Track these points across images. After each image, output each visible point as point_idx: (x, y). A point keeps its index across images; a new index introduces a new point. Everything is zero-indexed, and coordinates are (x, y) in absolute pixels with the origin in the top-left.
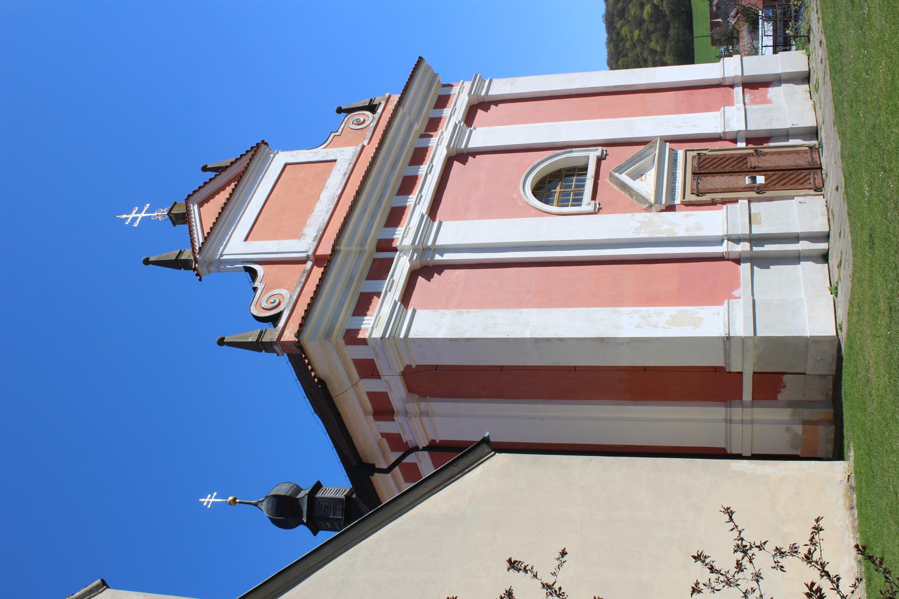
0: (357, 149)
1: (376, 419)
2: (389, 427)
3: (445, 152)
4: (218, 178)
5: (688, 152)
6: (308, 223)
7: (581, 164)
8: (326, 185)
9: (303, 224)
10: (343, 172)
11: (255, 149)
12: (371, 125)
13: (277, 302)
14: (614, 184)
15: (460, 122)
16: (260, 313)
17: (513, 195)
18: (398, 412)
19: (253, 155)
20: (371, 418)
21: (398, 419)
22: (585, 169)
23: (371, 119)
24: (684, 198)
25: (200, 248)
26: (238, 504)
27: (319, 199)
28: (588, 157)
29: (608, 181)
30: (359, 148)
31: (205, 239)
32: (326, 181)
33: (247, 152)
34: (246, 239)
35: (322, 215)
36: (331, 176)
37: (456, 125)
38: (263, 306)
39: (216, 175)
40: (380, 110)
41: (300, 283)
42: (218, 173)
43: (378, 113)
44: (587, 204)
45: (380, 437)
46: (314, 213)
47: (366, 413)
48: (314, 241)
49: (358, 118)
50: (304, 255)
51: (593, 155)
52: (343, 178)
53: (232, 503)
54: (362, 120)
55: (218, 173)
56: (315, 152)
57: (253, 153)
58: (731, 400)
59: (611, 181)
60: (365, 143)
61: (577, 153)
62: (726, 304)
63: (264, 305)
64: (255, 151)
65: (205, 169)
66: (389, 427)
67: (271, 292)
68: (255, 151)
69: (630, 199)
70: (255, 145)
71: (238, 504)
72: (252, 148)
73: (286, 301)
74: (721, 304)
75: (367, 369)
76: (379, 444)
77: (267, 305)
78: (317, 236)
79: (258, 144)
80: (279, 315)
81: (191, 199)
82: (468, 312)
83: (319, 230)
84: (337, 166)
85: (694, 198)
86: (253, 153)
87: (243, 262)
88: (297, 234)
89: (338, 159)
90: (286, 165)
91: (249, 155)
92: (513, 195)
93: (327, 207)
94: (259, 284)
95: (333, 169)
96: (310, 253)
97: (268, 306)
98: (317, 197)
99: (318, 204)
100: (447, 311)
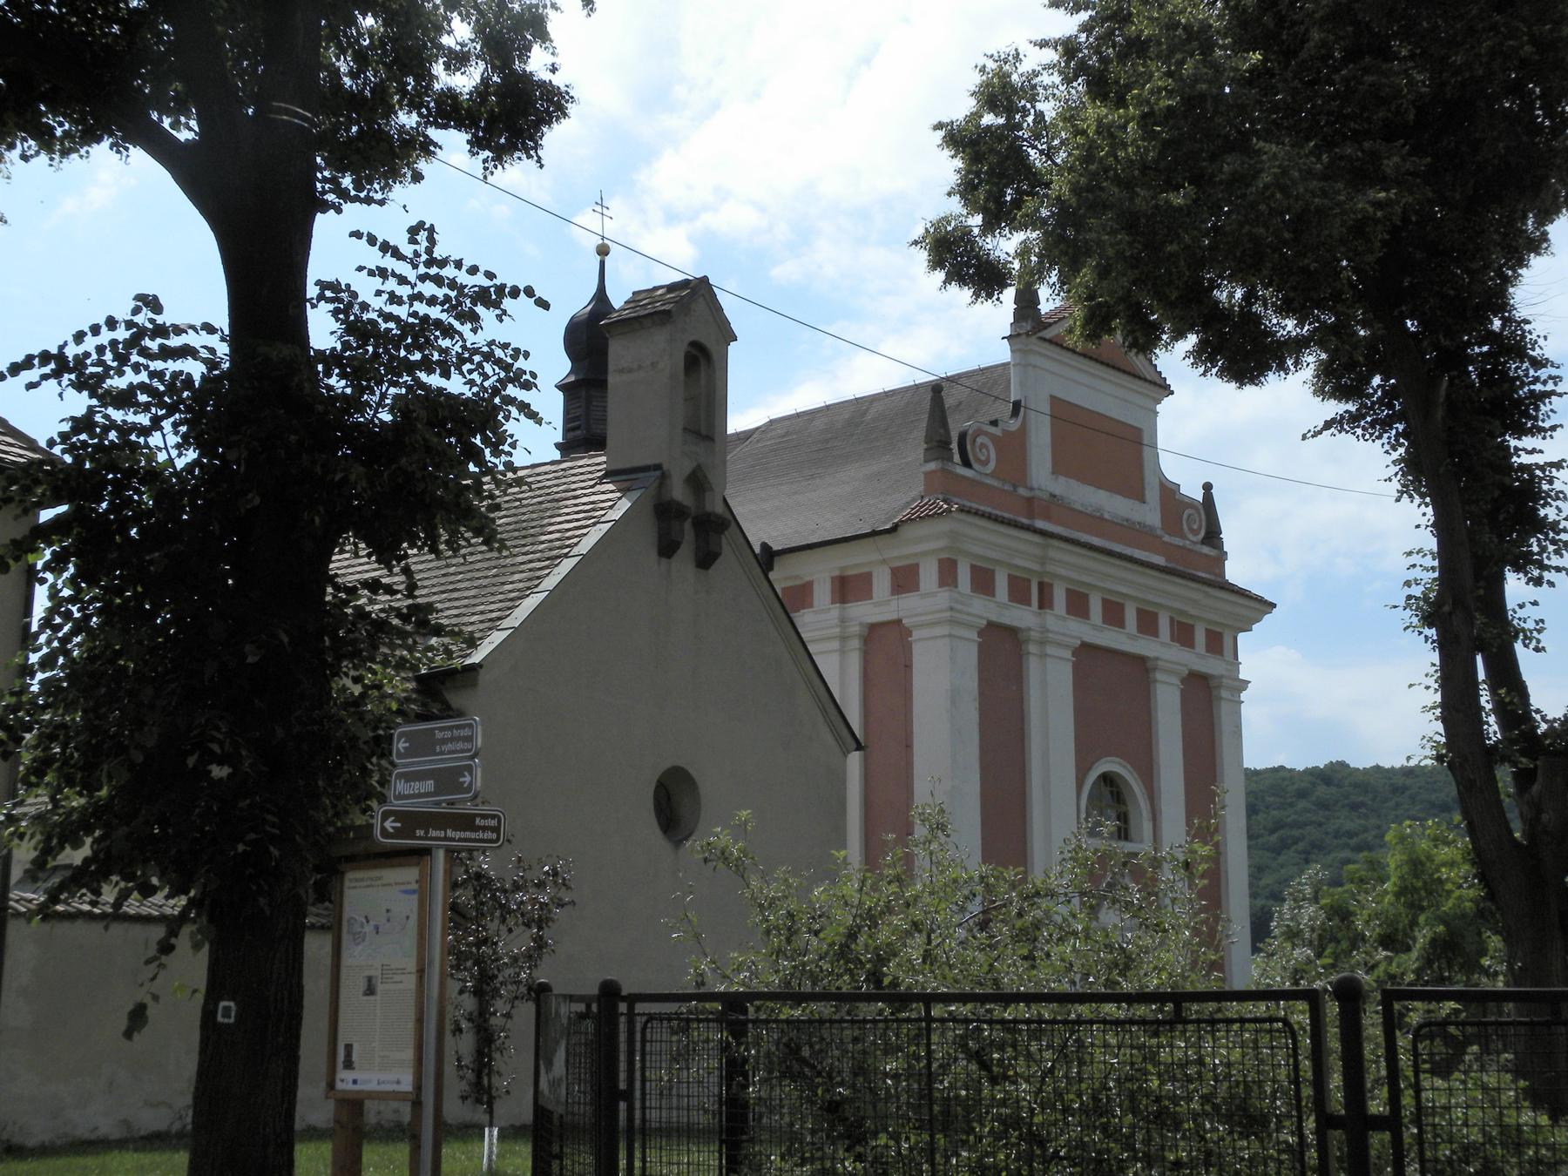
1: (833, 579)
2: (822, 593)
7: (1133, 832)
20: (837, 573)
21: (835, 611)
23: (1194, 539)
28: (1141, 841)
40: (1206, 550)
45: (807, 579)
47: (843, 569)
54: (1195, 527)
61: (1147, 827)
63: (979, 440)
64: (1160, 386)
66: (822, 593)
75: (904, 580)
76: (797, 577)
84: (1136, 505)
96: (1038, 493)
99: (1092, 489)
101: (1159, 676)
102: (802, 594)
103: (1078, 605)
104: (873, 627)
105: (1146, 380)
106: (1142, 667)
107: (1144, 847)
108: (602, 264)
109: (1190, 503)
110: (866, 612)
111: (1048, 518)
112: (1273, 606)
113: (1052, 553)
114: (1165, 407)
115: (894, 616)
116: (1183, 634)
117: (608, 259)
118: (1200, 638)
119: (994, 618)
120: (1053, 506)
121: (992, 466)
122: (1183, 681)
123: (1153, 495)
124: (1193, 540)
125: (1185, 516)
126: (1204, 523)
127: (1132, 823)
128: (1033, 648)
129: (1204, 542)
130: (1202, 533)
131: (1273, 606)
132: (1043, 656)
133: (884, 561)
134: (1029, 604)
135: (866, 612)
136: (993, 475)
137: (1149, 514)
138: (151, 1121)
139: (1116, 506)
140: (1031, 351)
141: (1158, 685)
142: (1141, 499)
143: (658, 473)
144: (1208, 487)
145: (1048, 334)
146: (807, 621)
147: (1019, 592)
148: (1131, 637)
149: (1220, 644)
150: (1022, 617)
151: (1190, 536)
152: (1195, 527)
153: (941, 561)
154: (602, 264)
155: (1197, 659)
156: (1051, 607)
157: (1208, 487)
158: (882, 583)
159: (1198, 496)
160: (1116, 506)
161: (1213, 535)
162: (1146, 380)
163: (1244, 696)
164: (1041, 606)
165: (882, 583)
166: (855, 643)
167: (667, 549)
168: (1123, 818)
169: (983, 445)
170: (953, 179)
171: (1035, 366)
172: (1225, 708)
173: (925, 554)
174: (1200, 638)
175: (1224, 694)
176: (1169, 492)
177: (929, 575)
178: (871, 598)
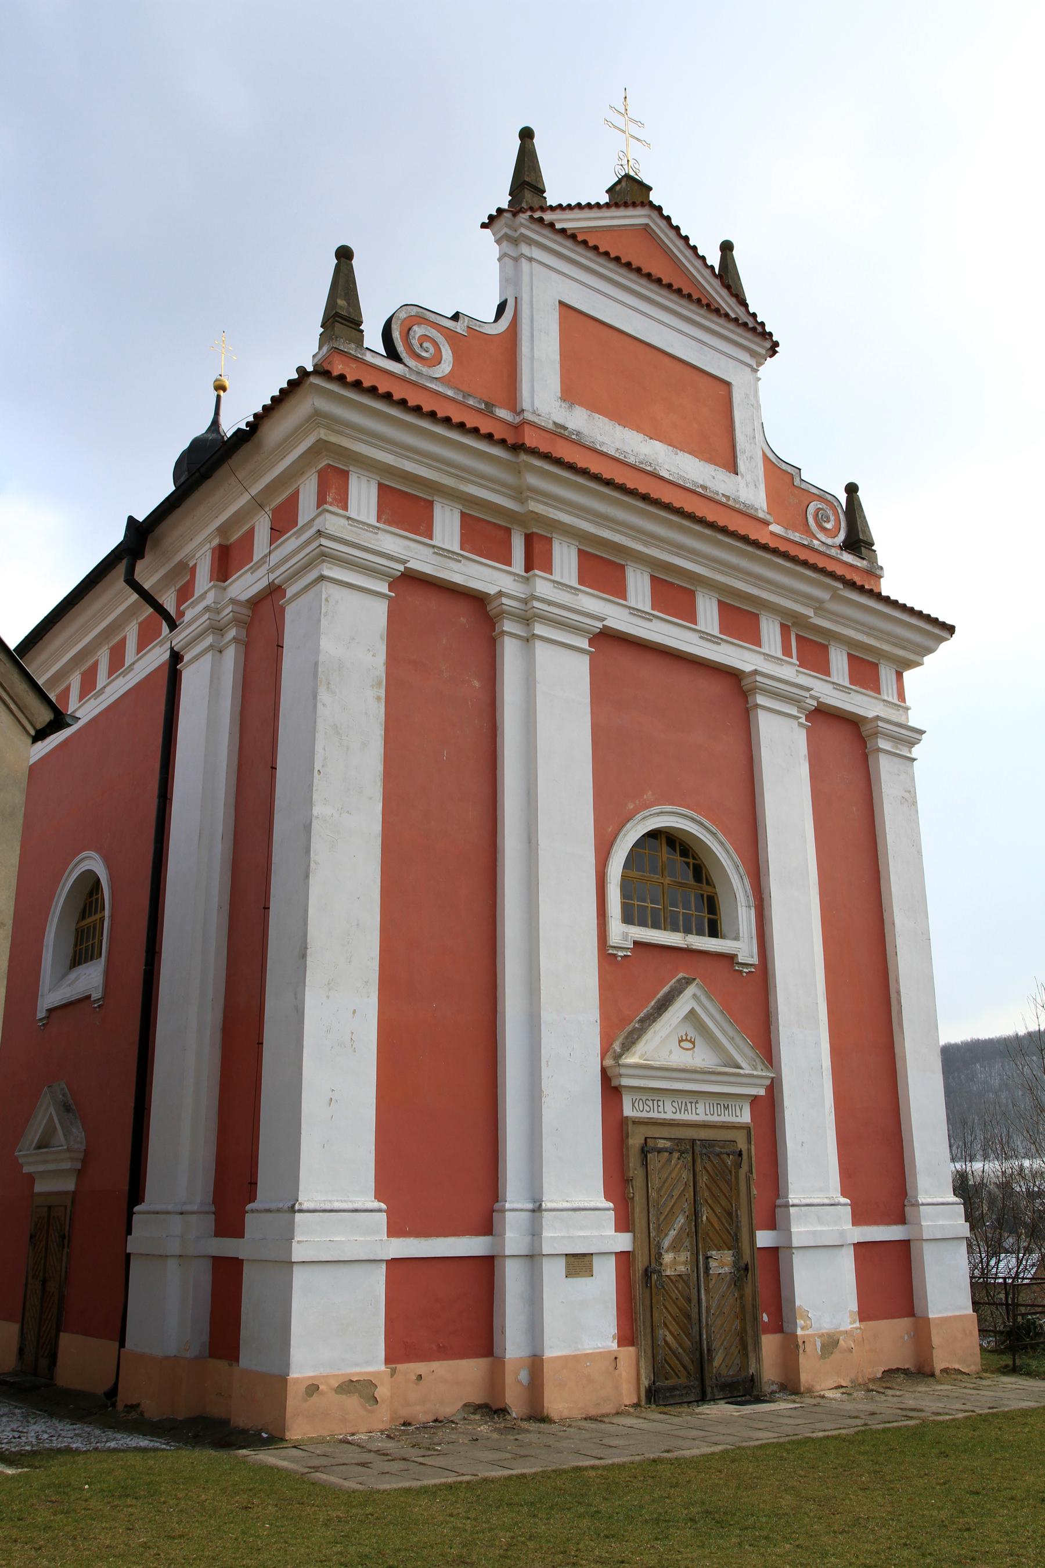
0: (759, 511)
1: (214, 550)
3: (748, 668)
4: (707, 273)
5: (744, 1132)
6: (597, 416)
7: (725, 925)
8: (680, 453)
9: (595, 407)
10: (708, 484)
11: (759, 329)
12: (816, 542)
13: (424, 354)
14: (671, 987)
15: (812, 697)
16: (399, 322)
17: (650, 792)
18: (225, 589)
19: (745, 324)
22: (714, 931)
23: (829, 541)
24: (634, 1122)
25: (552, 225)
26: (216, 393)
27: (651, 438)
28: (737, 938)
29: (680, 975)
30: (761, 515)
31: (563, 231)
32: (690, 454)
33: (754, 315)
34: (561, 303)
35: (613, 442)
36: (702, 462)
37: (809, 689)
38: (415, 328)
39: (712, 268)
40: (847, 557)
41: (464, 397)
42: (717, 271)
43: (841, 555)
44: (621, 933)
46: (619, 428)
48: (555, 423)
49: (832, 518)
50: (526, 404)
51: (745, 949)
52: (694, 483)
53: (218, 383)
54: (829, 526)
55: (717, 271)
56: (754, 437)
57: (751, 325)
58: (214, 1213)
59: (679, 981)
60: (775, 528)
61: (745, 918)
62: (377, 1205)
63: (418, 331)
64: (754, 329)
65: (727, 247)
67: (447, 345)
68: (754, 329)
69: (638, 1018)
70: (768, 329)
71: (216, 393)
72: (762, 324)
73: (425, 370)
74: (379, 1196)
77: (417, 337)
78: (565, 429)
79: (770, 334)
81: (655, 214)
82: (379, 699)
83: (578, 433)
85: (635, 1141)
86: (751, 325)
87: (516, 298)
88: (570, 395)
89: (739, 476)
90: (728, 384)
91: (744, 318)
92: (650, 792)
93: (632, 451)
94: (466, 324)
95: (717, 468)
96: (528, 416)
97: (414, 337)
98: (656, 434)
100: (381, 657)
109: (823, 496)
113: (532, 480)
125: (811, 509)
126: (843, 524)
128: (508, 626)
131: (951, 629)
132: (529, 640)
134: (509, 563)
138: (321, 1277)
140: (530, 242)
141: (760, 712)
144: (852, 489)
148: (705, 636)
151: (821, 536)
156: (548, 568)
157: (852, 489)
164: (528, 569)
168: (712, 905)
170: (809, 561)
171: (530, 259)
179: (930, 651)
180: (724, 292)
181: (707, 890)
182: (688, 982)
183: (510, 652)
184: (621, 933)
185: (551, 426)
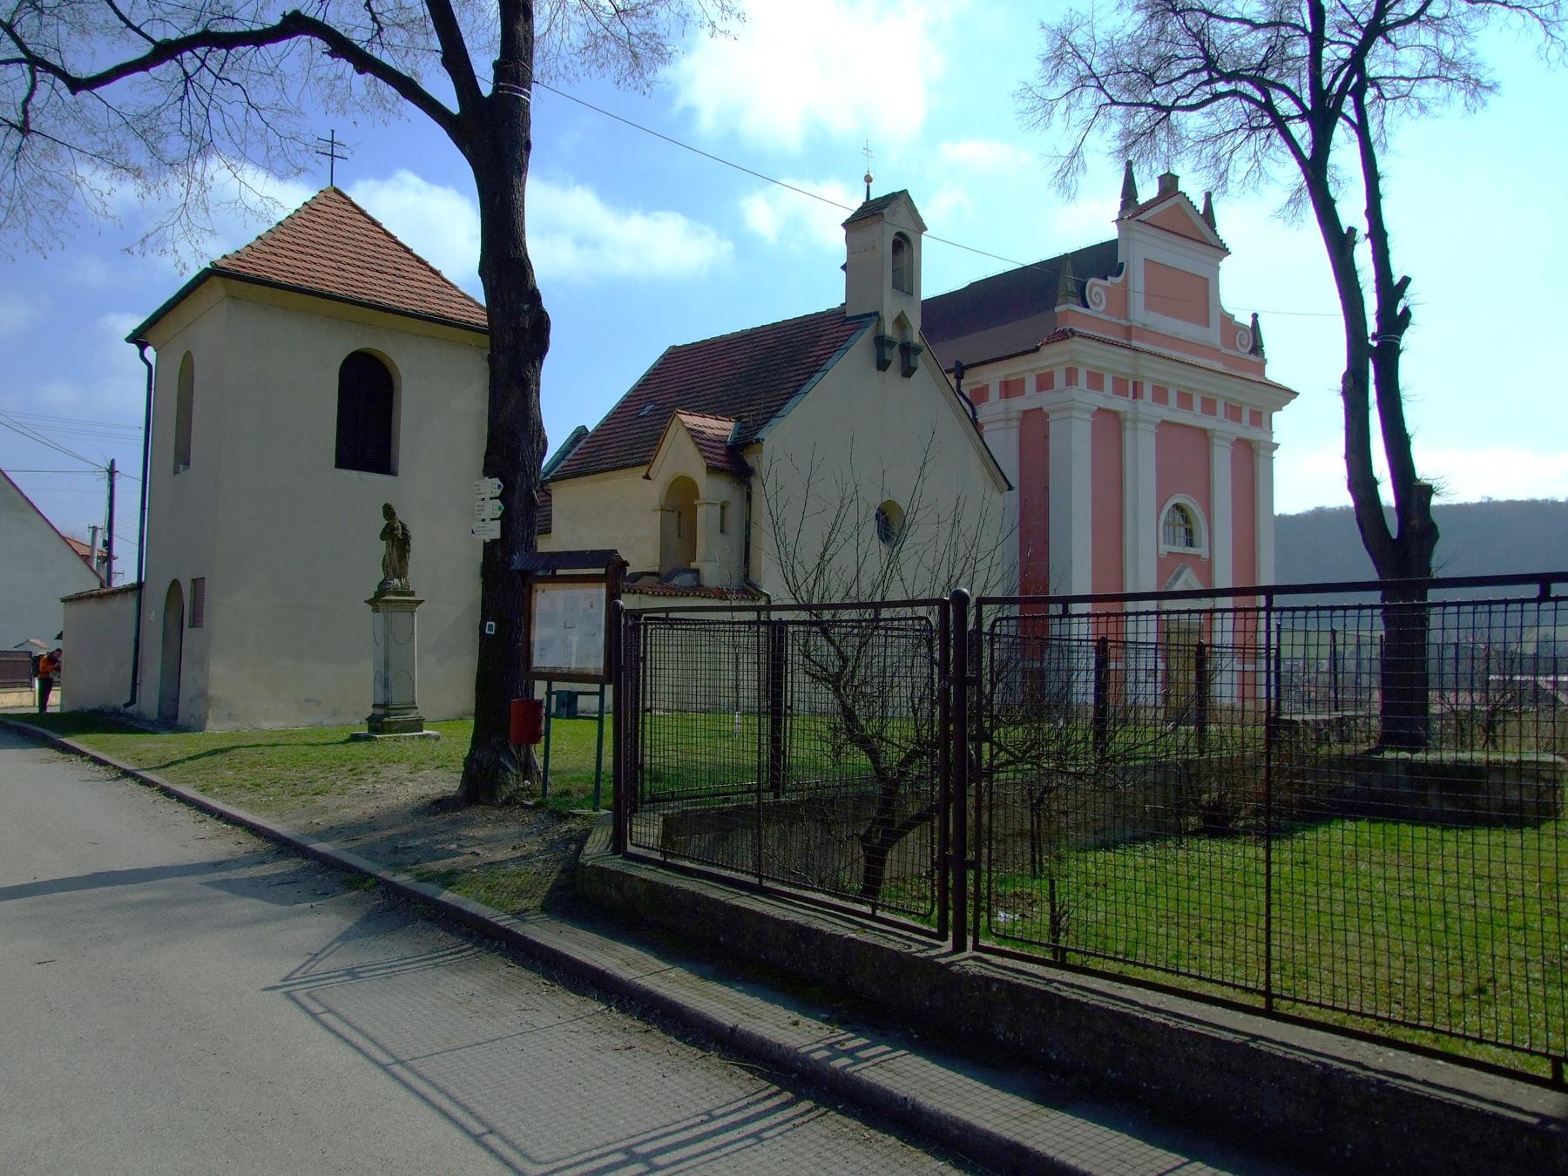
2: (994, 392)
21: (1003, 403)
28: (1200, 547)
30: (1218, 347)
40: (1252, 357)
50: (1132, 318)
54: (1245, 343)
63: (1094, 290)
66: (994, 392)
75: (1045, 383)
80: (1086, 306)
88: (1149, 307)
96: (1134, 323)
101: (1216, 441)
102: (981, 394)
103: (1160, 395)
104: (1026, 412)
105: (1211, 245)
106: (1204, 435)
107: (1201, 550)
108: (868, 187)
109: (1242, 327)
110: (1020, 404)
111: (1141, 339)
112: (1298, 394)
114: (1226, 265)
115: (1038, 406)
116: (1234, 413)
117: (871, 184)
118: (1246, 415)
119: (1102, 405)
120: (1145, 332)
121: (1102, 307)
122: (1233, 444)
123: (1215, 321)
124: (1243, 352)
125: (1239, 334)
126: (1251, 340)
127: (1195, 532)
128: (1128, 425)
129: (1251, 352)
130: (1250, 346)
133: (1032, 370)
134: (1127, 396)
135: (1020, 404)
136: (1105, 312)
137: (1213, 336)
139: (1188, 330)
142: (1206, 323)
143: (876, 318)
144: (1255, 316)
145: (1143, 217)
146: (984, 412)
147: (1120, 387)
149: (1261, 419)
150: (1119, 404)
152: (1245, 343)
153: (1067, 369)
154: (868, 187)
155: (1245, 431)
156: (1142, 398)
157: (1255, 316)
158: (1031, 385)
159: (1248, 322)
160: (1188, 330)
161: (1257, 348)
162: (1211, 245)
163: (1275, 454)
164: (1135, 397)
165: (1031, 385)
166: (1015, 423)
167: (882, 365)
168: (1189, 532)
169: (1098, 293)
172: (1261, 462)
173: (1057, 364)
174: (1246, 415)
175: (1262, 452)
176: (1228, 320)
177: (1060, 378)
178: (1024, 394)
179: (1287, 403)
180: (1206, 226)
181: (1189, 527)
182: (1186, 567)
183: (1128, 434)
184: (1165, 549)
185: (1141, 326)
